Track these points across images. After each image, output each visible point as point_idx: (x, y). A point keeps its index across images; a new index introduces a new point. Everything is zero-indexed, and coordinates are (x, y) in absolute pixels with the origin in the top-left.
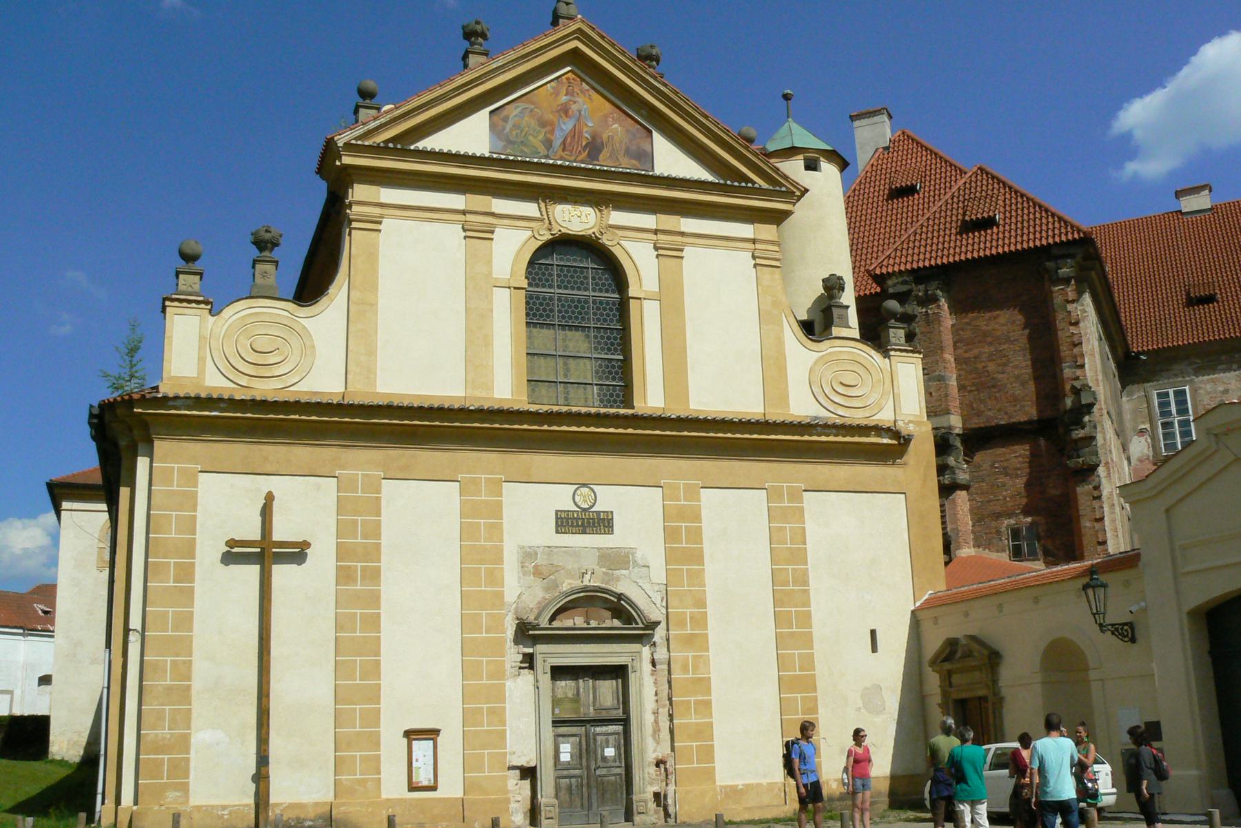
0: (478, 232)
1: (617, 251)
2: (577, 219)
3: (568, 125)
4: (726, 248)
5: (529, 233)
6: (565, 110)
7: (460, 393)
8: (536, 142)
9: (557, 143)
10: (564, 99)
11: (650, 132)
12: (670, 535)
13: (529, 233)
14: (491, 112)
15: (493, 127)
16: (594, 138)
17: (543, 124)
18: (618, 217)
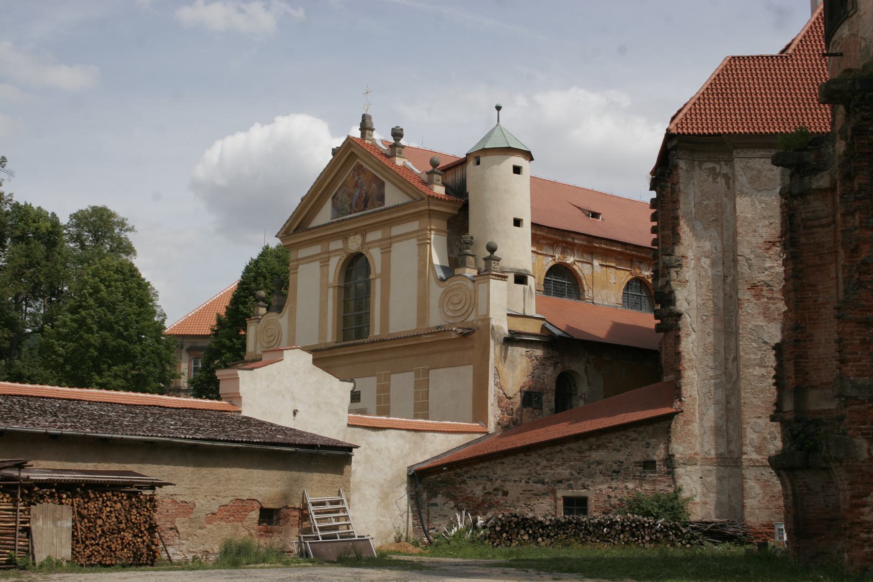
0: (325, 263)
1: (367, 256)
2: (354, 244)
3: (357, 194)
4: (408, 239)
5: (338, 258)
6: (356, 185)
7: (316, 343)
8: (347, 206)
9: (354, 204)
10: (356, 178)
11: (383, 183)
12: (379, 399)
13: (338, 258)
14: (333, 198)
15: (334, 205)
16: (367, 194)
17: (349, 196)
18: (372, 236)
